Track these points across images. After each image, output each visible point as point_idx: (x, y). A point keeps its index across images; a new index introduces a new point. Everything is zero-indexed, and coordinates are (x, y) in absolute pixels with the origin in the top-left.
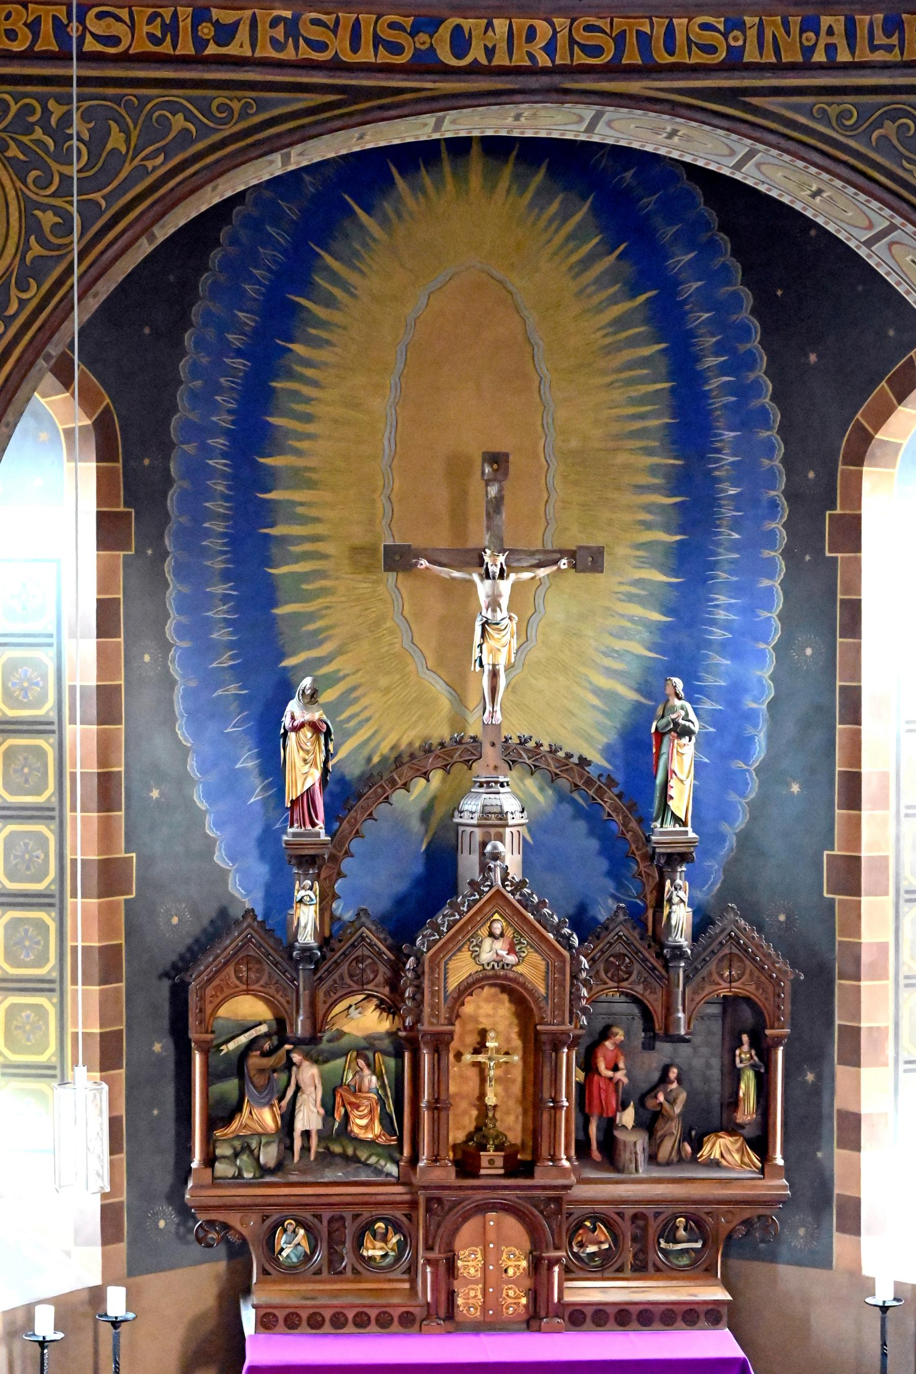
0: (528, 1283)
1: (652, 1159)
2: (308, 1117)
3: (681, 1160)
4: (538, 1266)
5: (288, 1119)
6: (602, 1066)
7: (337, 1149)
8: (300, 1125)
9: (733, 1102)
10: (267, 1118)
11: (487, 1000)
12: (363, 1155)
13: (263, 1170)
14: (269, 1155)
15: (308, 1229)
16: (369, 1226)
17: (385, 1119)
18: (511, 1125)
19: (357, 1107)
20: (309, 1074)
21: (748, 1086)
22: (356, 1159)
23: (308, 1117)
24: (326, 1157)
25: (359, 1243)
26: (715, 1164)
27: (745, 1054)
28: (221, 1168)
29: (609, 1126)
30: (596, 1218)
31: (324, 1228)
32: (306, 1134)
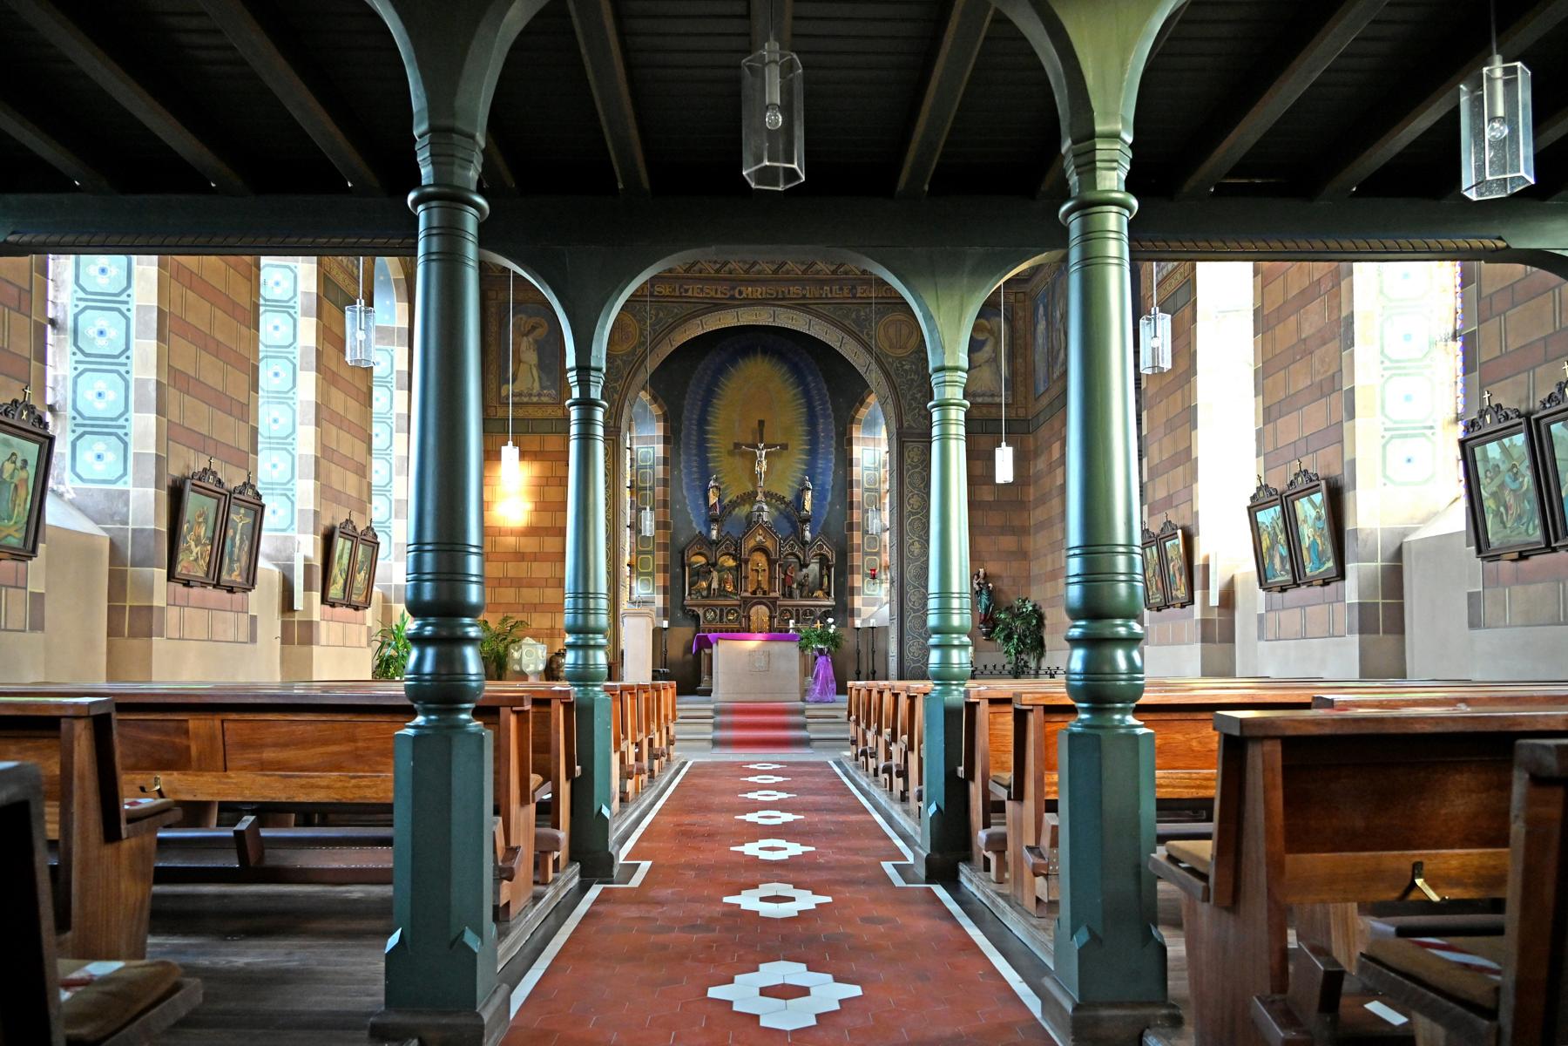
2: (715, 585)
4: (771, 618)
9: (821, 584)
10: (704, 584)
18: (765, 586)
20: (715, 574)
23: (715, 585)
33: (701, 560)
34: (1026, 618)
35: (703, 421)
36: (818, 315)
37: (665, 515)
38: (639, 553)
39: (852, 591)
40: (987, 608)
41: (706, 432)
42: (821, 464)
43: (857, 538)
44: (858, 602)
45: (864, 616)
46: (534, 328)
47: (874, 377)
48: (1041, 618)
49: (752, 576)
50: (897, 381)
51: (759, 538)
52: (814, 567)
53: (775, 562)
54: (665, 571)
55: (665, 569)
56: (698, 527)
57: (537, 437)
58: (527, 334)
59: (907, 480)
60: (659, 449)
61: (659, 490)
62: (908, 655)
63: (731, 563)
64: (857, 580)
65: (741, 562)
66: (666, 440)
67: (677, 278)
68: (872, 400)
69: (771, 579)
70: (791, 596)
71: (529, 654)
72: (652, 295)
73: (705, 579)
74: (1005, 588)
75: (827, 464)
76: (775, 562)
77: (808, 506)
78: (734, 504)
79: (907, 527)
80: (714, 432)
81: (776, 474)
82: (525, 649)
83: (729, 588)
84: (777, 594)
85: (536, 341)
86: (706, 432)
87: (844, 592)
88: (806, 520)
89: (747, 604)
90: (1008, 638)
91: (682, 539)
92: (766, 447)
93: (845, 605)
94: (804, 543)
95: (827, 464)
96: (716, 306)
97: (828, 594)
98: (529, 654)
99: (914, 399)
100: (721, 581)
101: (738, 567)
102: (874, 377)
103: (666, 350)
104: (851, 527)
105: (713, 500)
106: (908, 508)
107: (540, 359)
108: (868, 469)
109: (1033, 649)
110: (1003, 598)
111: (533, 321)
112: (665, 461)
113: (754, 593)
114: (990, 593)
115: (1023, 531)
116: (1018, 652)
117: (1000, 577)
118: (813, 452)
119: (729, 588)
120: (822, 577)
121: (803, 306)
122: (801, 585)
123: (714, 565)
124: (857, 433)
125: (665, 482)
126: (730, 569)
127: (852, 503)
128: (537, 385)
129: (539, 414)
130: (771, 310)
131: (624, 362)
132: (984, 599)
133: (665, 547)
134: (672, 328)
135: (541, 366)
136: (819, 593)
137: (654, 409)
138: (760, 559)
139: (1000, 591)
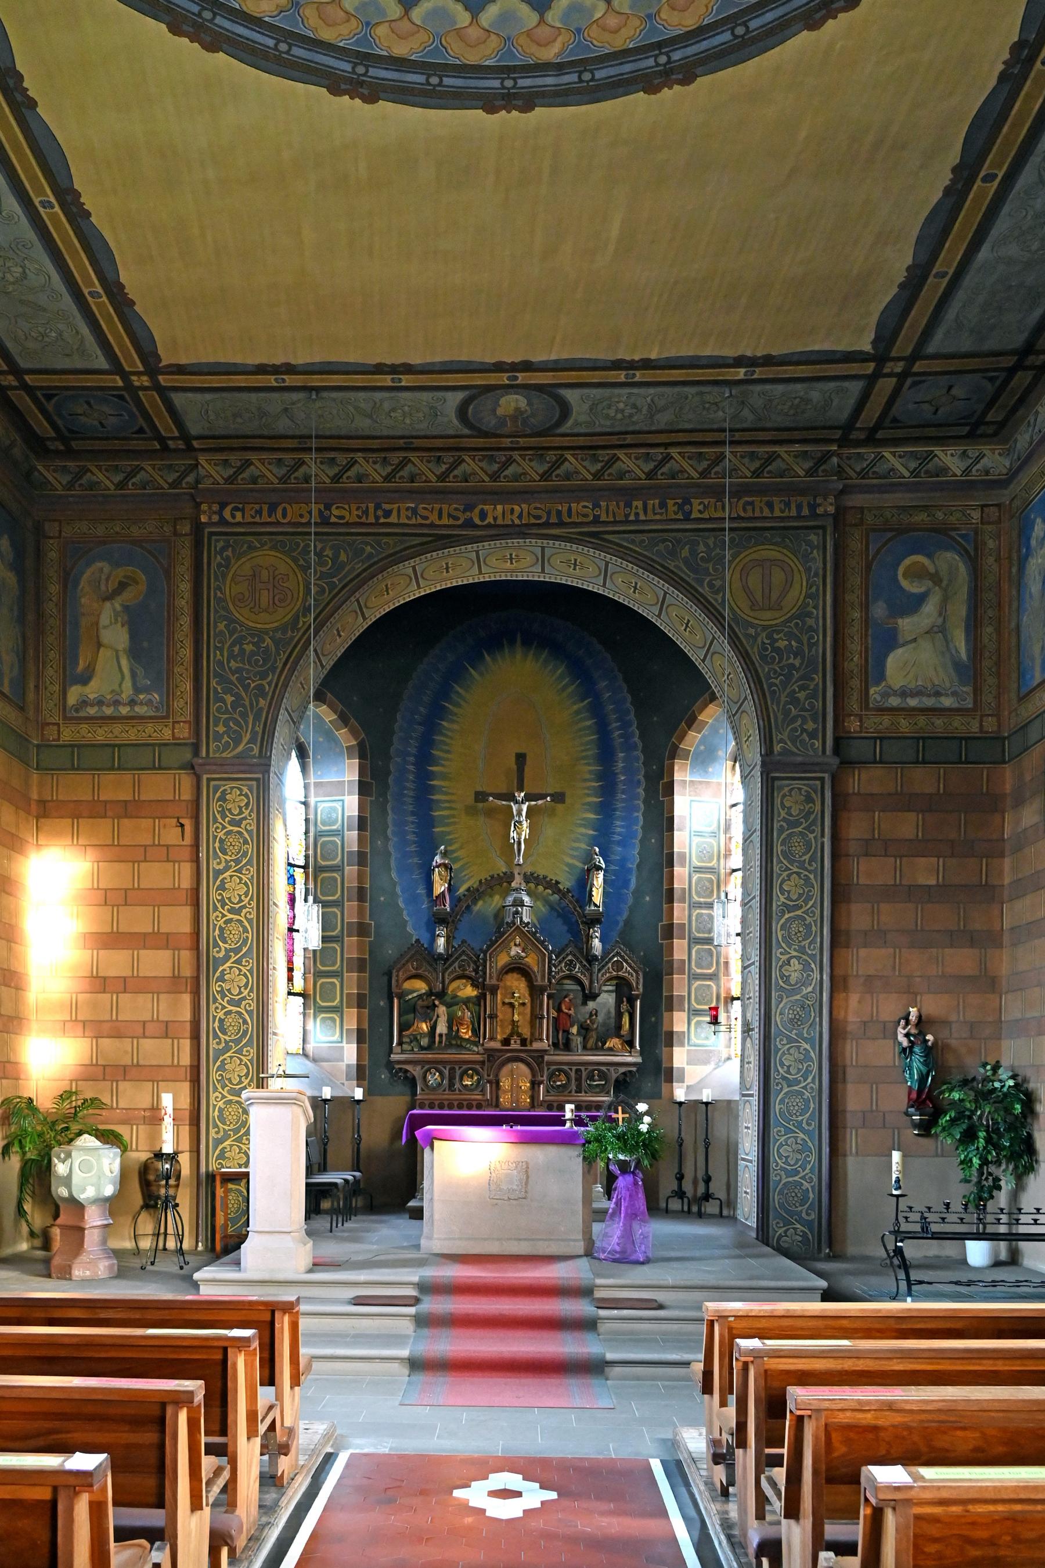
0: (530, 1093)
1: (585, 1048)
2: (442, 1028)
3: (597, 1048)
4: (534, 1084)
5: (433, 1028)
6: (563, 1008)
7: (454, 1042)
8: (438, 1031)
9: (619, 1027)
10: (424, 1027)
11: (516, 980)
12: (464, 1044)
13: (422, 1048)
14: (425, 1042)
15: (441, 1074)
16: (465, 1072)
17: (474, 1031)
18: (525, 1031)
19: (462, 1024)
20: (442, 1010)
21: (626, 1019)
22: (461, 1046)
23: (442, 1028)
24: (449, 1046)
25: (461, 1079)
26: (610, 1049)
27: (624, 1006)
28: (405, 1046)
29: (567, 1032)
30: (559, 1070)
31: (446, 1072)
32: (441, 1035)
33: (421, 986)
34: (1004, 1100)
35: (425, 758)
36: (624, 553)
37: (361, 912)
38: (318, 974)
39: (670, 1039)
40: (923, 1079)
41: (431, 776)
42: (619, 827)
43: (680, 949)
44: (679, 1057)
45: (689, 1080)
46: (122, 586)
47: (720, 665)
48: (1029, 1101)
49: (502, 1013)
50: (764, 670)
51: (515, 951)
52: (607, 999)
53: (542, 990)
54: (360, 1005)
55: (360, 1002)
56: (415, 931)
57: (127, 777)
58: (109, 597)
59: (778, 848)
60: (351, 803)
61: (351, 870)
62: (776, 1161)
63: (469, 991)
64: (679, 1022)
65: (486, 990)
66: (363, 789)
67: (372, 490)
68: (711, 715)
69: (536, 1018)
70: (567, 1047)
71: (85, 1167)
72: (325, 522)
73: (426, 1018)
74: (953, 1043)
75: (628, 825)
76: (542, 990)
77: (597, 896)
78: (475, 894)
79: (778, 934)
80: (444, 777)
81: (539, 841)
82: (77, 1157)
83: (466, 1033)
84: (544, 1045)
85: (126, 608)
86: (431, 776)
87: (657, 1041)
88: (594, 920)
89: (494, 1061)
90: (969, 1136)
91: (390, 951)
92: (528, 798)
93: (658, 1063)
94: (591, 959)
95: (628, 825)
96: (440, 540)
97: (631, 1043)
98: (85, 1167)
99: (794, 701)
100: (451, 1022)
101: (482, 997)
102: (720, 665)
103: (350, 626)
104: (669, 931)
105: (440, 887)
106: (779, 899)
107: (133, 636)
108: (699, 834)
109: (1013, 1157)
110: (951, 1060)
111: (120, 573)
112: (362, 823)
113: (506, 1042)
114: (929, 1052)
115: (988, 940)
116: (985, 1162)
117: (945, 1023)
118: (606, 809)
119: (466, 1033)
120: (619, 1015)
121: (594, 537)
122: (585, 1030)
123: (441, 995)
124: (682, 774)
125: (361, 858)
126: (467, 1001)
127: (671, 891)
128: (128, 684)
129: (132, 734)
130: (535, 544)
131: (277, 642)
132: (917, 1063)
133: (360, 965)
134: (361, 581)
135: (135, 652)
136: (613, 1042)
137: (344, 737)
138: (518, 986)
139: (946, 1047)
